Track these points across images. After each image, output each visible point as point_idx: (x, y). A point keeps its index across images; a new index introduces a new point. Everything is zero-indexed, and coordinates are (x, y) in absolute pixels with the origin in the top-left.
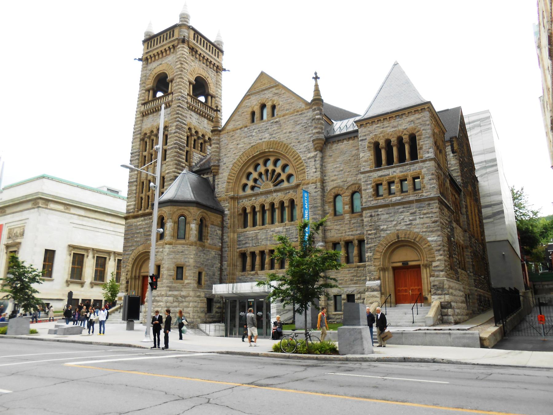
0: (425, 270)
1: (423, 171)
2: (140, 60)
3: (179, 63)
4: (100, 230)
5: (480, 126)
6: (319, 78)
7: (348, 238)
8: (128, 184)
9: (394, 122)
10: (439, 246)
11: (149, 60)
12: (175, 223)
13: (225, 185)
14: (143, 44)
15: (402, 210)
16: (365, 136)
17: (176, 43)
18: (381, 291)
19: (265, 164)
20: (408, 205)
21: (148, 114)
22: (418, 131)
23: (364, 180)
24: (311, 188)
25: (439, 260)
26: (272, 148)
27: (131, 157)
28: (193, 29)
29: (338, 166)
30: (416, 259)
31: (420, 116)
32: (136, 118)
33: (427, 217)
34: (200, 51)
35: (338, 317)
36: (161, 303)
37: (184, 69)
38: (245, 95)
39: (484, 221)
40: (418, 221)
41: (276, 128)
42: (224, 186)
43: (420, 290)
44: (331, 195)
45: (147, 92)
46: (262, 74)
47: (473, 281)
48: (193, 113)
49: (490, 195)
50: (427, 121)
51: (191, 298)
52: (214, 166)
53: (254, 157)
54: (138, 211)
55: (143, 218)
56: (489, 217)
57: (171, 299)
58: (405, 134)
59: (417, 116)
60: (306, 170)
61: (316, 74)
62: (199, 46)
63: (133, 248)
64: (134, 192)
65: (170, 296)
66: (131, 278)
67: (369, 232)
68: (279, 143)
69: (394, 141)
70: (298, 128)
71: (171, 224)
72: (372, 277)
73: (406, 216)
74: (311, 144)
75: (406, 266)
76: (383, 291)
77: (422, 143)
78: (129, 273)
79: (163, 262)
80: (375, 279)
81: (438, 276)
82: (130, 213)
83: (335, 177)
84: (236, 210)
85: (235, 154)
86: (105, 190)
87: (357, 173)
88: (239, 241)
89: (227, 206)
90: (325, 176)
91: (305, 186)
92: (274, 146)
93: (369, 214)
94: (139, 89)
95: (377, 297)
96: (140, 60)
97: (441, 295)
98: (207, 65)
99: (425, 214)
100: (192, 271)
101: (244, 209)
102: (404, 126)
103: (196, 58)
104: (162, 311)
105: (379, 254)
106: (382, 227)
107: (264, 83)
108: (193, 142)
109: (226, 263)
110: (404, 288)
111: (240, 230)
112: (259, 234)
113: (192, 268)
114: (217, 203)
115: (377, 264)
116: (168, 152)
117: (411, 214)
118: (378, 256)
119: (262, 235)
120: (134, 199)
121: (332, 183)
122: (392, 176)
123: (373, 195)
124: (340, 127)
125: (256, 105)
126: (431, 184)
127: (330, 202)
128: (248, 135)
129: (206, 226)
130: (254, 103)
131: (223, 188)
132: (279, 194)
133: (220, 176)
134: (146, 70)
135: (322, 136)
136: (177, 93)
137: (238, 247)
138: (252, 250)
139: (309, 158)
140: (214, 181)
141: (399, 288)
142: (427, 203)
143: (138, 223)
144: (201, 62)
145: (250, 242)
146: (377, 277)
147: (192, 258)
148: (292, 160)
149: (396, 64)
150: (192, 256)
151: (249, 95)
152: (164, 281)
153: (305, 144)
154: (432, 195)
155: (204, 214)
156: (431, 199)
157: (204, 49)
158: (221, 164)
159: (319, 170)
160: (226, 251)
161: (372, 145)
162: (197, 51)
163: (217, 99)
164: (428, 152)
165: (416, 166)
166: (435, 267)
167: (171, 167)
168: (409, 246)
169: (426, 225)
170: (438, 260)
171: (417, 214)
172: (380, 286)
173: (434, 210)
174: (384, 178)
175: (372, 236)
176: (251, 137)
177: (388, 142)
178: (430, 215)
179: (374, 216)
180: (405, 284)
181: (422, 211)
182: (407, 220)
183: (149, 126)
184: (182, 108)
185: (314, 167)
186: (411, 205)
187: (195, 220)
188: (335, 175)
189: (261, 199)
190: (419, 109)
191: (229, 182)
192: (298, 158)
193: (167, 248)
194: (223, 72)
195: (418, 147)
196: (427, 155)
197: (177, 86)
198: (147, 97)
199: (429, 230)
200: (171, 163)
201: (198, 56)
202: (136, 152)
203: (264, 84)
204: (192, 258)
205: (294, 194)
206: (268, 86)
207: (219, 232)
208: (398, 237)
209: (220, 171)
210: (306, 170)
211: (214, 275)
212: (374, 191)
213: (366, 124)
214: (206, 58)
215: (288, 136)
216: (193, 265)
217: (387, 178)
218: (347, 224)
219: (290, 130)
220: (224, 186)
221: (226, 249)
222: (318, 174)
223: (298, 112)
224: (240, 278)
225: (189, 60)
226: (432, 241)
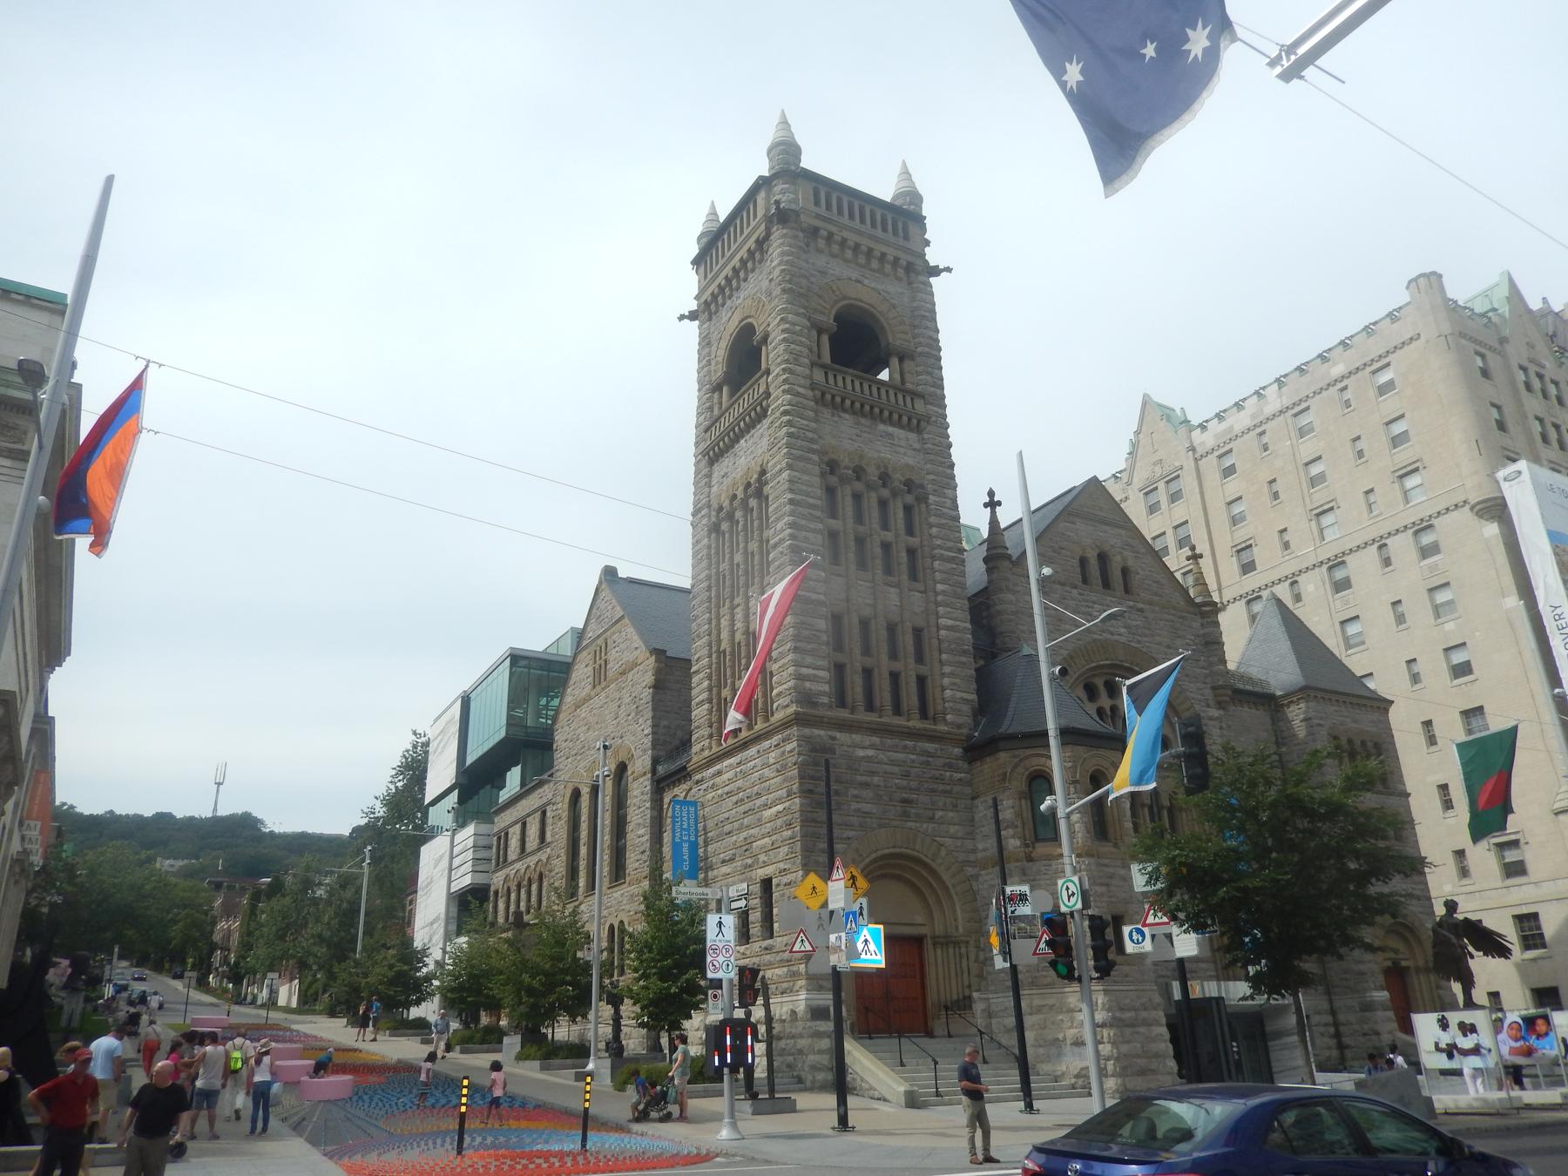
45: (814, 333)
55: (876, 740)
63: (851, 834)
139: (1211, 719)
143: (861, 753)
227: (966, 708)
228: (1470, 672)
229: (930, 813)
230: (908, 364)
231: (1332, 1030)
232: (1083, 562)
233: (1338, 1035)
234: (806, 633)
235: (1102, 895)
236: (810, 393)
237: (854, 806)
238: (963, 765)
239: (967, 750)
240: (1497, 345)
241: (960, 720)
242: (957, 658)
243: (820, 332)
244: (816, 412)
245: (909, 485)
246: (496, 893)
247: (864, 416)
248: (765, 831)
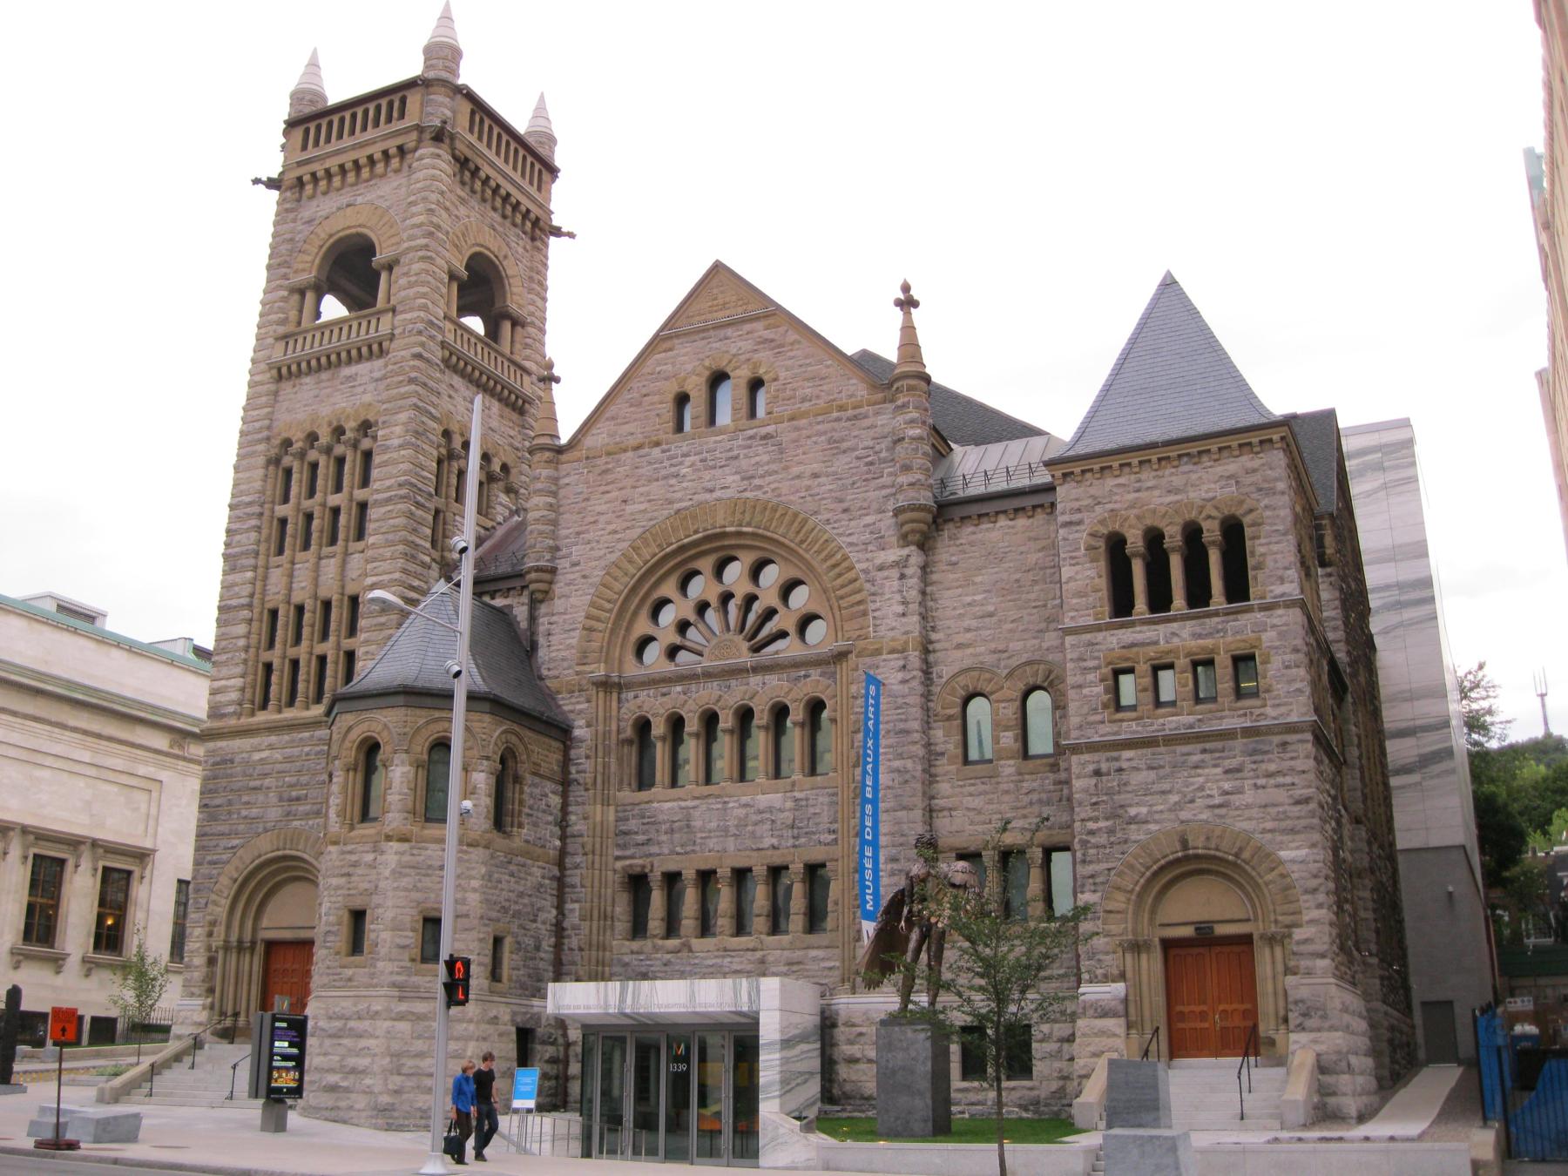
0: (1267, 951)
1: (1264, 636)
2: (272, 184)
3: (420, 208)
4: (49, 761)
5: (1380, 467)
6: (915, 304)
8: (215, 613)
9: (1174, 476)
10: (1315, 876)
11: (309, 188)
12: (418, 765)
13: (574, 639)
14: (286, 133)
15: (1196, 758)
16: (1079, 510)
17: (410, 140)
18: (1127, 1015)
19: (719, 571)
20: (1219, 745)
21: (300, 373)
22: (1251, 511)
23: (1075, 655)
24: (890, 672)
25: (1315, 924)
26: (749, 525)
27: (231, 520)
28: (470, 97)
29: (978, 598)
30: (1237, 917)
31: (1256, 463)
32: (252, 385)
33: (1277, 786)
34: (486, 170)
35: (973, 1097)
36: (371, 1042)
37: (438, 227)
38: (656, 336)
39: (1394, 781)
40: (1249, 796)
41: (765, 458)
42: (574, 642)
43: (1252, 1014)
44: (953, 692)
45: (296, 297)
46: (718, 269)
47: (1377, 981)
48: (457, 381)
49: (1411, 696)
50: (1276, 480)
51: (472, 1027)
52: (538, 569)
53: (682, 549)
54: (253, 714)
55: (273, 739)
56: (1405, 770)
57: (404, 1026)
58: (1209, 517)
59: (1246, 461)
60: (872, 606)
61: (906, 288)
62: (486, 151)
63: (236, 842)
64: (242, 642)
65: (401, 1017)
66: (227, 948)
67: (1091, 825)
68: (774, 510)
69: (1173, 536)
70: (841, 463)
71: (406, 768)
72: (1099, 972)
73: (1211, 779)
74: (887, 522)
75: (1205, 938)
76: (1133, 1018)
77: (1262, 550)
78: (220, 931)
79: (376, 899)
80: (1107, 979)
81: (1309, 973)
82: (224, 716)
83: (969, 635)
84: (614, 727)
85: (615, 532)
86: (51, 607)
87: (1043, 625)
88: (625, 833)
89: (581, 712)
90: (933, 629)
91: (868, 660)
92: (758, 518)
93: (1091, 767)
94: (262, 283)
95: (1115, 1035)
96: (272, 184)
97: (1319, 1030)
98: (504, 217)
99: (1270, 775)
100: (474, 934)
101: (643, 726)
102: (1203, 490)
103: (473, 191)
104: (376, 1068)
105: (1121, 897)
106: (1133, 811)
107: (722, 303)
108: (454, 481)
109: (576, 906)
110: (1197, 1009)
111: (627, 795)
112: (696, 813)
113: (476, 922)
114: (549, 697)
115: (1114, 929)
116: (373, 513)
117: (1226, 772)
118: (1119, 901)
119: (705, 815)
120: (239, 670)
121: (958, 654)
122: (1169, 646)
123: (1105, 706)
124: (975, 467)
125: (693, 372)
126: (1290, 682)
127: (949, 718)
128: (664, 472)
129: (517, 779)
130: (689, 367)
131: (570, 647)
132: (772, 680)
133: (559, 605)
134: (294, 221)
135: (925, 498)
136: (412, 310)
137: (618, 853)
138: (672, 867)
139: (881, 568)
140: (532, 619)
141: (1179, 1008)
142: (1277, 739)
143: (257, 756)
144: (488, 206)
145: (664, 838)
146: (1116, 972)
147: (475, 890)
148: (821, 568)
149: (1169, 285)
150: (475, 883)
151: (670, 337)
152: (380, 965)
153: (869, 519)
154: (1294, 718)
155: (514, 739)
156: (1291, 728)
157: (499, 162)
158: (562, 564)
159: (914, 607)
160: (577, 867)
161: (1101, 544)
162: (477, 169)
163: (530, 329)
164: (1282, 580)
165: (1245, 619)
166: (1298, 943)
167: (386, 565)
168: (1217, 873)
169: (1273, 811)
170: (1311, 922)
171: (1246, 774)
172: (1126, 1000)
173: (1300, 764)
174: (1141, 650)
175: (1102, 839)
176: (673, 481)
177: (1154, 538)
178: (1288, 780)
179: (1108, 774)
180: (1208, 995)
181: (1264, 766)
182: (1215, 792)
183: (300, 416)
184: (428, 361)
185: (898, 597)
186: (1231, 743)
187: (487, 758)
188: (968, 630)
189: (705, 695)
190: (1255, 440)
191: (591, 630)
192: (841, 565)
193: (393, 853)
194: (553, 240)
195: (1251, 562)
196: (1278, 589)
197: (411, 285)
198: (293, 314)
199: (1284, 825)
200: (387, 552)
201: (478, 185)
202: (250, 504)
203: (724, 306)
204: (475, 890)
205: (825, 681)
206: (739, 313)
207: (555, 800)
208: (1185, 845)
209: (558, 588)
210: (873, 606)
211: (538, 948)
212: (1106, 691)
213: (1083, 472)
214: (503, 192)
215: (808, 488)
216: (479, 912)
217: (1151, 652)
218: (1007, 792)
219: (816, 467)
220: (574, 642)
221: (578, 859)
222: (913, 621)
223: (841, 408)
224: (626, 959)
225: (454, 199)
226: (1293, 861)
229: (315, 808)
235: (338, 888)
237: (244, 813)
242: (375, 621)
245: (366, 427)
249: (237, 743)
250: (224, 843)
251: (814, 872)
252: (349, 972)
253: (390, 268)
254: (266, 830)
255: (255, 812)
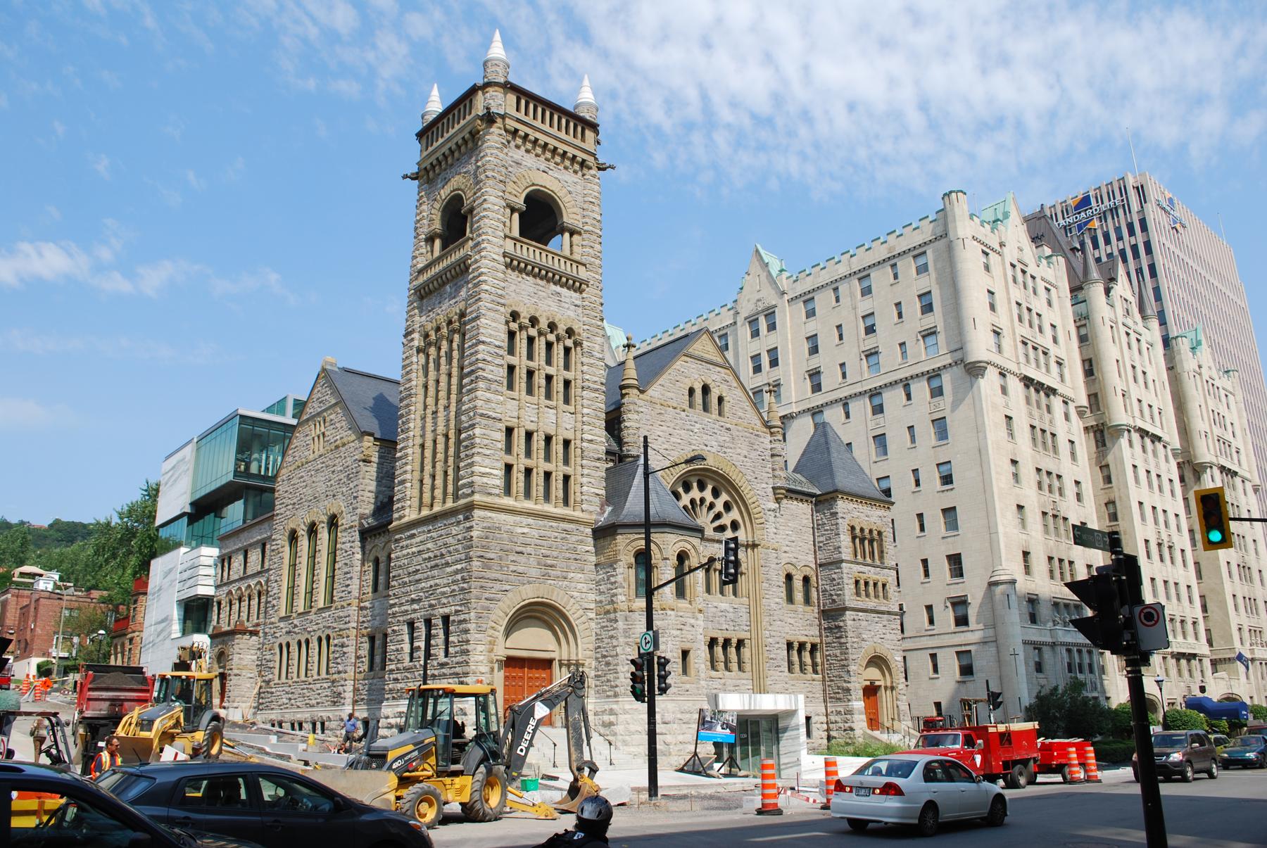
7: (803, 639)
45: (508, 211)
55: (530, 521)
63: (508, 587)
70: (754, 455)
82: (490, 494)
143: (520, 530)
219: (745, 453)
227: (597, 500)
228: (951, 482)
230: (576, 237)
231: (825, 726)
232: (691, 391)
233: (828, 730)
234: (486, 442)
236: (501, 259)
237: (512, 568)
238: (590, 540)
239: (595, 531)
240: (997, 247)
241: (591, 508)
243: (513, 210)
244: (504, 273)
245: (570, 332)
246: (219, 603)
247: (542, 279)
248: (445, 581)
249: (502, 516)
250: (498, 586)
251: (740, 643)
252: (688, 686)
253: (572, 234)
254: (529, 583)
255: (520, 569)
